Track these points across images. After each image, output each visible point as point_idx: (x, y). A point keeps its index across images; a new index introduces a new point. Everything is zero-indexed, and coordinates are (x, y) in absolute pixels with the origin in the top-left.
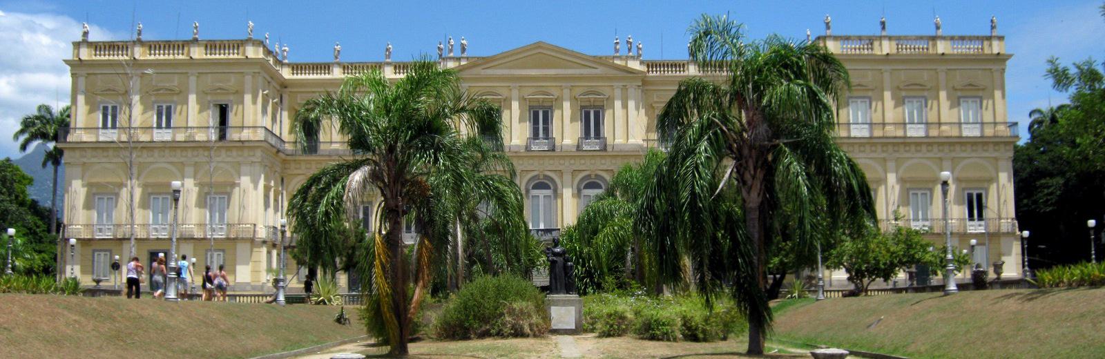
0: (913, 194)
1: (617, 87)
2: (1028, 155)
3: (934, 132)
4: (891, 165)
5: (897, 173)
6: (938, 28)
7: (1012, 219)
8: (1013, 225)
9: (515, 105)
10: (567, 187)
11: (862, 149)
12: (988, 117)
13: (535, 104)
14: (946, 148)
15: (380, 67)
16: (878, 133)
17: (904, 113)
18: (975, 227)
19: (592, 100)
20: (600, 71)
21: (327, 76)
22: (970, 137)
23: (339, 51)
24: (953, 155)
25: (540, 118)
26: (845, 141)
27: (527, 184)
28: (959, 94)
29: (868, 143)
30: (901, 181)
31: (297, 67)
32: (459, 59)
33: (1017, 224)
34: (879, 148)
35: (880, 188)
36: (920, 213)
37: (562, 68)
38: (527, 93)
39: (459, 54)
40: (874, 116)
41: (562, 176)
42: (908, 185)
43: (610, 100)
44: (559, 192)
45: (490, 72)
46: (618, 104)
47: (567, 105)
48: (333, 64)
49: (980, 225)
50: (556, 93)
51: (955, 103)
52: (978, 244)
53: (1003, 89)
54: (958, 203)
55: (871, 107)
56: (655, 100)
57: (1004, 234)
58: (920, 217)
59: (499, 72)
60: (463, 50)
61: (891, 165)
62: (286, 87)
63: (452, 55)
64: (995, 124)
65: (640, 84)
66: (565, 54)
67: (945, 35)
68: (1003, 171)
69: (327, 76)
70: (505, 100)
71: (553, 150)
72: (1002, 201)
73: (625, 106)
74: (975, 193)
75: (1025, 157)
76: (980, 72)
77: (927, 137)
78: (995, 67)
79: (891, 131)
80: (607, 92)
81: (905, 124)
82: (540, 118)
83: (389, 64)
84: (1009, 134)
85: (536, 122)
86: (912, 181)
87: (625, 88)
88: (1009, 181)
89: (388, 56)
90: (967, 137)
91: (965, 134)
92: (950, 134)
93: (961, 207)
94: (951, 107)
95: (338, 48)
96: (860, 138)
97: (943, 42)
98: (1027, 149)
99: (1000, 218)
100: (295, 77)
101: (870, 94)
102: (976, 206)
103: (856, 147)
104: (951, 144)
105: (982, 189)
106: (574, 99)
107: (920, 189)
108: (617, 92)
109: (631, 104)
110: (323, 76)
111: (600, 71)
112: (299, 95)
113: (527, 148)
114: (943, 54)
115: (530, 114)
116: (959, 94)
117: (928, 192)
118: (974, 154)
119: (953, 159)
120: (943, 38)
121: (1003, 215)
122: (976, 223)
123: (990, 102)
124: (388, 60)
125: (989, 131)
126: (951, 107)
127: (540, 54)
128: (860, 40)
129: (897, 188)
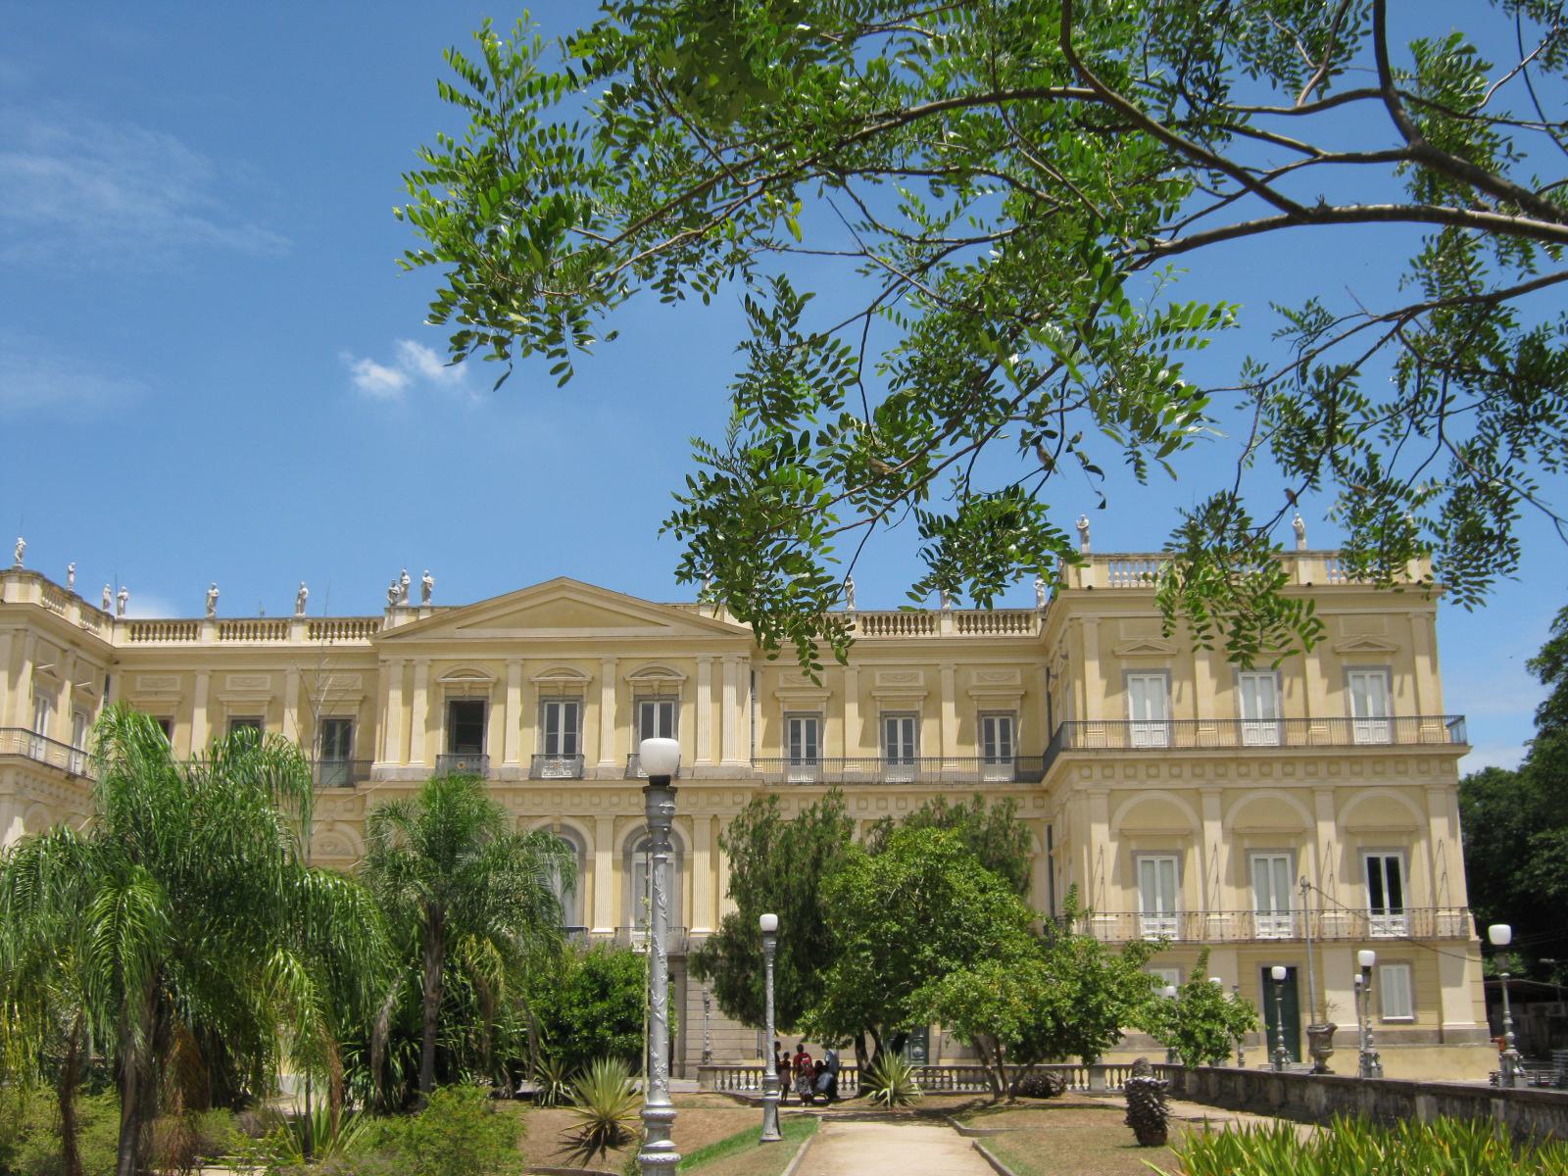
0: (1144, 862)
1: (705, 660)
2: (1519, 788)
3: (1297, 738)
4: (1211, 803)
5: (1223, 819)
6: (1299, 536)
7: (1462, 910)
8: (1464, 922)
9: (514, 695)
10: (604, 849)
11: (1153, 771)
12: (1404, 707)
13: (552, 692)
14: (1322, 768)
15: (285, 626)
16: (1184, 739)
17: (1236, 700)
18: (1388, 926)
19: (656, 684)
20: (672, 630)
21: (191, 643)
22: (1369, 746)
23: (215, 599)
24: (1338, 781)
25: (560, 718)
26: (1118, 756)
27: (626, 841)
28: (1345, 662)
29: (1164, 760)
30: (1233, 834)
31: (141, 628)
32: (416, 610)
33: (1471, 920)
34: (1187, 771)
35: (1190, 851)
36: (1159, 901)
37: (591, 626)
38: (536, 671)
39: (418, 602)
40: (1176, 708)
41: (593, 829)
42: (1247, 844)
43: (690, 683)
44: (588, 857)
45: (469, 633)
46: (704, 693)
47: (609, 695)
48: (202, 621)
49: (1394, 923)
50: (588, 671)
51: (1338, 680)
52: (1379, 962)
53: (1432, 652)
54: (1351, 878)
55: (1169, 692)
56: (781, 685)
57: (1443, 939)
58: (1273, 907)
59: (487, 633)
60: (427, 594)
61: (1211, 803)
62: (117, 663)
63: (405, 602)
64: (1419, 719)
65: (747, 654)
66: (610, 600)
67: (1313, 548)
68: (1439, 815)
69: (191, 643)
70: (496, 685)
71: (580, 778)
72: (1438, 873)
73: (717, 697)
74: (1383, 858)
75: (1513, 792)
76: (1385, 619)
77: (1283, 747)
78: (1416, 609)
79: (1209, 736)
80: (684, 669)
81: (1238, 721)
82: (560, 718)
83: (300, 621)
84: (1448, 740)
85: (552, 726)
86: (1252, 833)
87: (717, 662)
88: (1453, 835)
89: (301, 608)
90: (1363, 746)
91: (1358, 739)
92: (1327, 741)
93: (1356, 888)
94: (1330, 690)
95: (213, 593)
96: (1148, 750)
97: (1310, 563)
98: (1519, 776)
99: (1436, 910)
100: (136, 644)
101: (1168, 664)
102: (1385, 882)
103: (1142, 770)
104: (1331, 760)
105: (1397, 849)
106: (621, 684)
107: (1271, 850)
108: (704, 670)
109: (730, 693)
110: (184, 643)
111: (672, 630)
112: (139, 678)
113: (534, 776)
114: (1309, 584)
115: (541, 711)
116: (1345, 662)
117: (1288, 857)
118: (1377, 781)
119: (1336, 790)
120: (1311, 555)
121: (1443, 902)
122: (1387, 917)
123: (1408, 679)
124: (299, 615)
125: (1407, 734)
126: (1330, 690)
127: (559, 599)
128: (1147, 561)
129: (1225, 851)
